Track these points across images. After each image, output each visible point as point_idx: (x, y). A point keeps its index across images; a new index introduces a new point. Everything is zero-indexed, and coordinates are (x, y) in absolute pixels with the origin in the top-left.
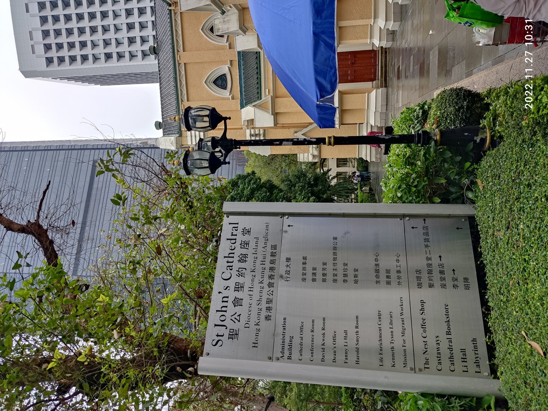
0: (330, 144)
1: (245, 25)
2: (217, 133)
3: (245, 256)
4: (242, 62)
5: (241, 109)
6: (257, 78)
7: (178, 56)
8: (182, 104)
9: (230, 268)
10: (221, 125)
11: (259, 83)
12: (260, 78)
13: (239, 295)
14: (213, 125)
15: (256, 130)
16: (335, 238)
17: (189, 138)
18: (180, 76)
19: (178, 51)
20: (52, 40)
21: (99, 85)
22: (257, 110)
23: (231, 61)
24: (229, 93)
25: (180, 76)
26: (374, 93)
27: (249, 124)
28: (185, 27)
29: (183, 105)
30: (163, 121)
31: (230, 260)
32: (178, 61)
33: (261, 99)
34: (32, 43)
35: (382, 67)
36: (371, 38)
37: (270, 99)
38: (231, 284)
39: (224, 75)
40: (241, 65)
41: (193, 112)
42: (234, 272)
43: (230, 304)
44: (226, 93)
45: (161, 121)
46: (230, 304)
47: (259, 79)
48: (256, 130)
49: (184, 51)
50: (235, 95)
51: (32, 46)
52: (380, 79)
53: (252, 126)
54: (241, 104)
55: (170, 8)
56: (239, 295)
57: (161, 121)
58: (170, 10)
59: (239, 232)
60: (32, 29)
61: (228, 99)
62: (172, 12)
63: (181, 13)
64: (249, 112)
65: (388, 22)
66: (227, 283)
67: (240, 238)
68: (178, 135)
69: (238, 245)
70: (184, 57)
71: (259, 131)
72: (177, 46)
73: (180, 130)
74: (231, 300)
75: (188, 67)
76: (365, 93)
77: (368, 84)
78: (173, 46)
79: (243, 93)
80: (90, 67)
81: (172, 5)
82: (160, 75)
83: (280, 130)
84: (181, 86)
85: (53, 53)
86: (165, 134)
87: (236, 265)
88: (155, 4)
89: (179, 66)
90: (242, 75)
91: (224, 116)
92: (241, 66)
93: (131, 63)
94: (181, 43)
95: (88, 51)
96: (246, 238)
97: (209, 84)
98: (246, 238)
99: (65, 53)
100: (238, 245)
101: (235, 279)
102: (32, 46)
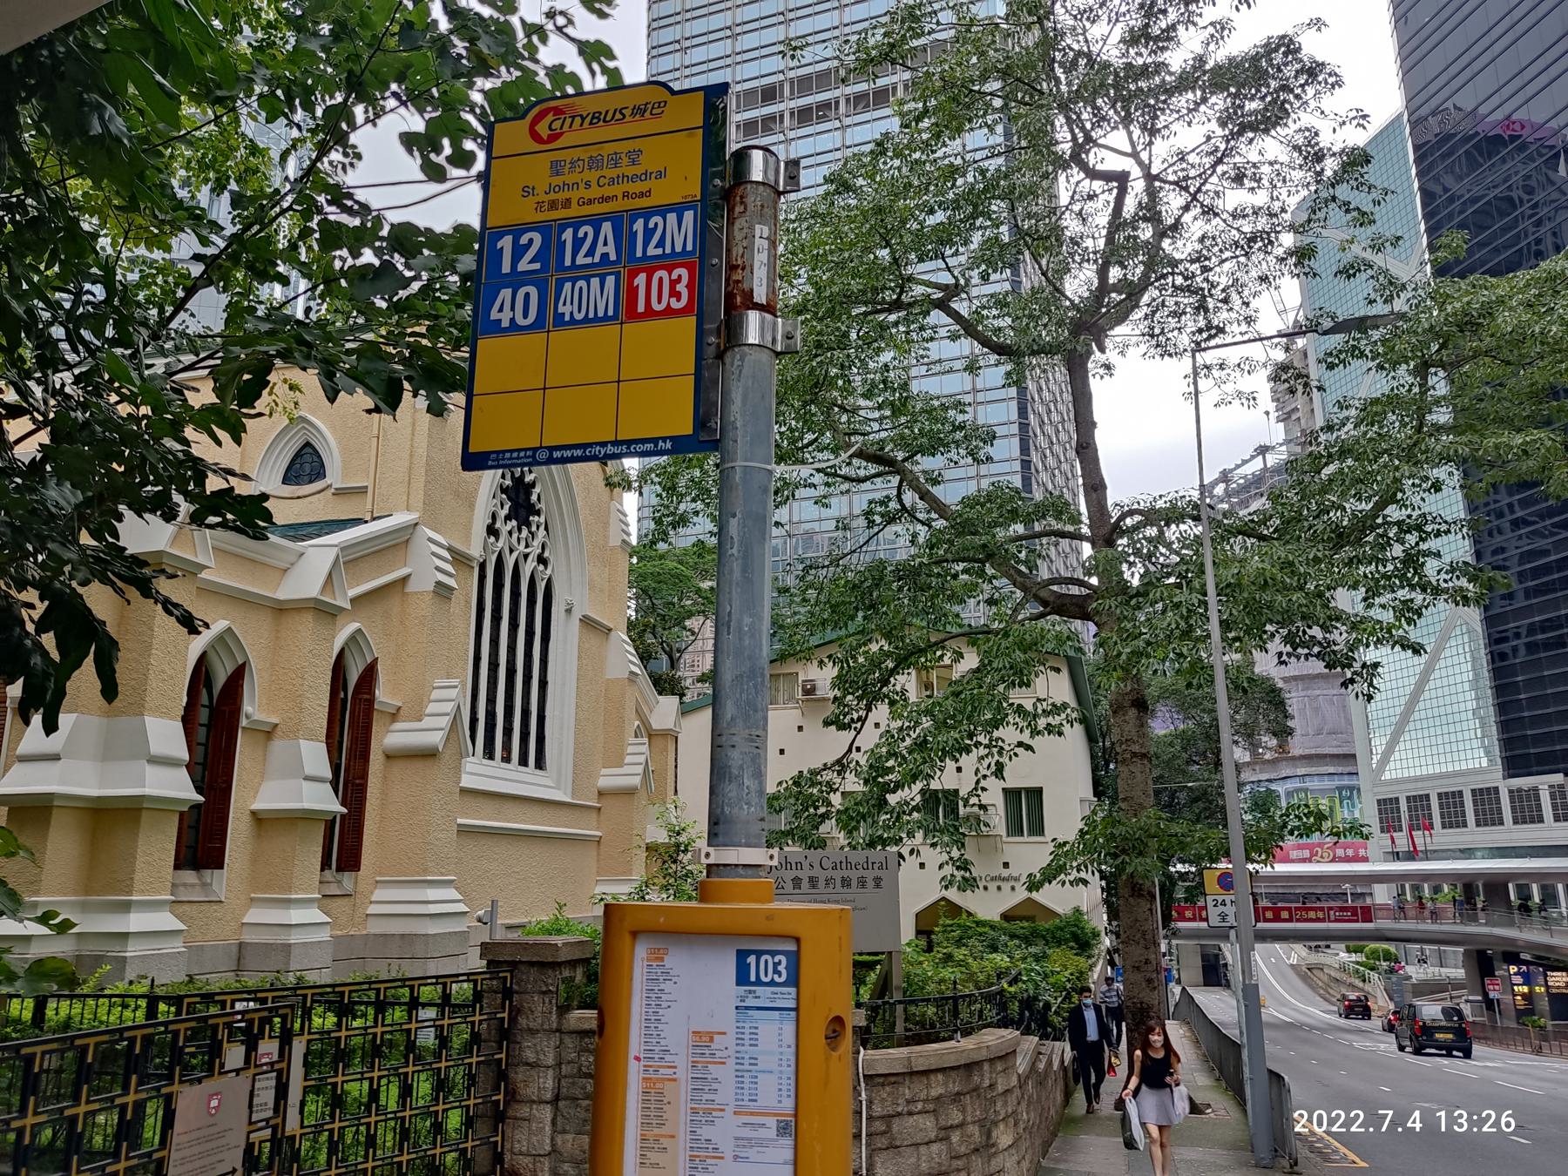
3: (849, 885)
9: (834, 868)
13: (805, 884)
31: (844, 865)
38: (817, 872)
42: (830, 873)
43: (794, 873)
46: (794, 873)
56: (805, 884)
59: (877, 873)
66: (816, 865)
67: (870, 875)
69: (861, 873)
74: (799, 874)
87: (838, 875)
96: (870, 884)
100: (861, 873)
101: (822, 876)
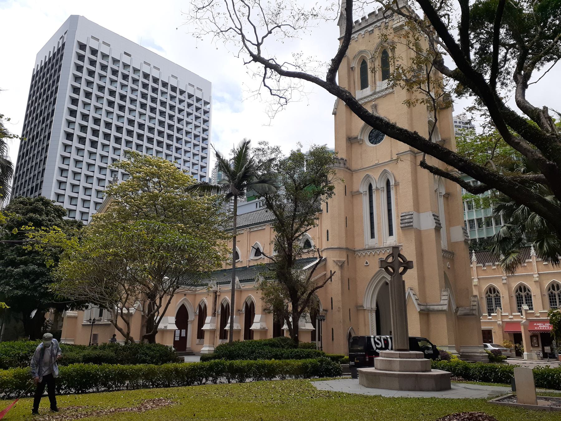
85: (87, 54)
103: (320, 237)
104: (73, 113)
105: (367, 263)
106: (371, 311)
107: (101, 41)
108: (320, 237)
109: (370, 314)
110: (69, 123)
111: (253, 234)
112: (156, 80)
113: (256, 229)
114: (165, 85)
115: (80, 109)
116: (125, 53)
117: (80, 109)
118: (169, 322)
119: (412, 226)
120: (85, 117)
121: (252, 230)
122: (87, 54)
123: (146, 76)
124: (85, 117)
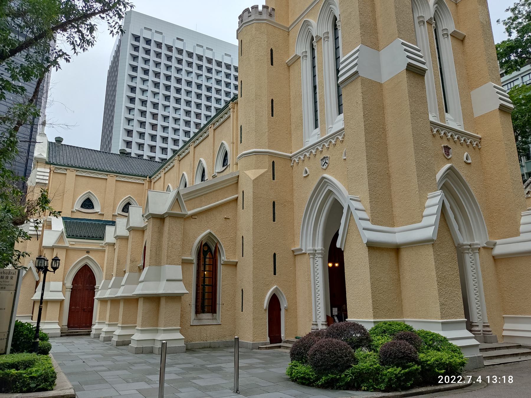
0: (40, 306)
1: (118, 239)
2: (49, 268)
4: (101, 223)
5: (62, 217)
6: (85, 236)
7: (113, 176)
8: (74, 170)
10: (52, 270)
11: (81, 237)
12: (84, 239)
14: (52, 267)
15: (41, 228)
16: (5, 309)
17: (43, 170)
18: (98, 173)
19: (117, 176)
20: (153, 48)
21: (109, 69)
22: (60, 233)
23: (103, 215)
24: (77, 209)
25: (98, 173)
26: (57, 326)
27: (47, 223)
28: (134, 185)
29: (73, 170)
30: (62, 144)
31: (2, 273)
32: (110, 175)
33: (67, 237)
34: (153, 31)
35: (77, 332)
36: (98, 322)
37: (66, 245)
39: (93, 208)
40: (99, 221)
41: (58, 261)
44: (77, 206)
45: (62, 143)
47: (84, 238)
48: (41, 228)
49: (116, 180)
50: (75, 214)
51: (151, 30)
52: (69, 331)
53: (45, 224)
54: (66, 217)
55: (148, 177)
57: (62, 143)
58: (146, 177)
60: (164, 36)
61: (73, 208)
62: (146, 178)
63: (144, 184)
64: (58, 225)
65: (105, 333)
68: (47, 161)
70: (112, 179)
71: (40, 231)
72: (121, 176)
73: (52, 164)
75: (104, 181)
76: (59, 320)
77: (65, 322)
78: (121, 174)
79: (75, 221)
80: (125, 71)
81: (150, 179)
82: (103, 152)
83: (38, 249)
84: (90, 172)
85: (142, 44)
86: (50, 143)
88: (156, 162)
89: (105, 174)
90: (91, 222)
91: (55, 271)
92: (98, 221)
93: (124, 108)
94: (123, 180)
95: (140, 74)
97: (88, 194)
98: (9, 278)
99: (141, 54)
102: (151, 30)
103: (235, 141)
104: (132, 100)
105: (306, 172)
106: (314, 255)
107: (153, 31)
108: (235, 141)
109: (311, 259)
110: (130, 110)
111: (182, 161)
112: (210, 61)
113: (184, 154)
114: (219, 64)
115: (138, 95)
116: (178, 39)
117: (138, 95)
118: (51, 289)
119: (356, 72)
120: (144, 102)
121: (181, 157)
122: (142, 44)
123: (200, 58)
124: (144, 102)
